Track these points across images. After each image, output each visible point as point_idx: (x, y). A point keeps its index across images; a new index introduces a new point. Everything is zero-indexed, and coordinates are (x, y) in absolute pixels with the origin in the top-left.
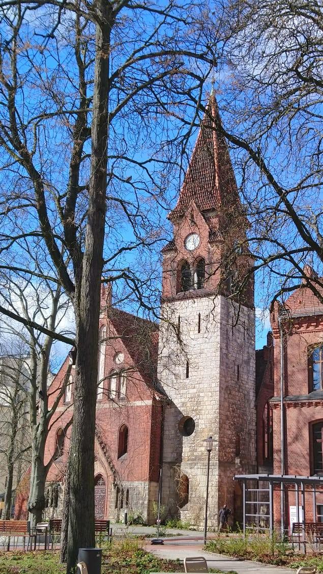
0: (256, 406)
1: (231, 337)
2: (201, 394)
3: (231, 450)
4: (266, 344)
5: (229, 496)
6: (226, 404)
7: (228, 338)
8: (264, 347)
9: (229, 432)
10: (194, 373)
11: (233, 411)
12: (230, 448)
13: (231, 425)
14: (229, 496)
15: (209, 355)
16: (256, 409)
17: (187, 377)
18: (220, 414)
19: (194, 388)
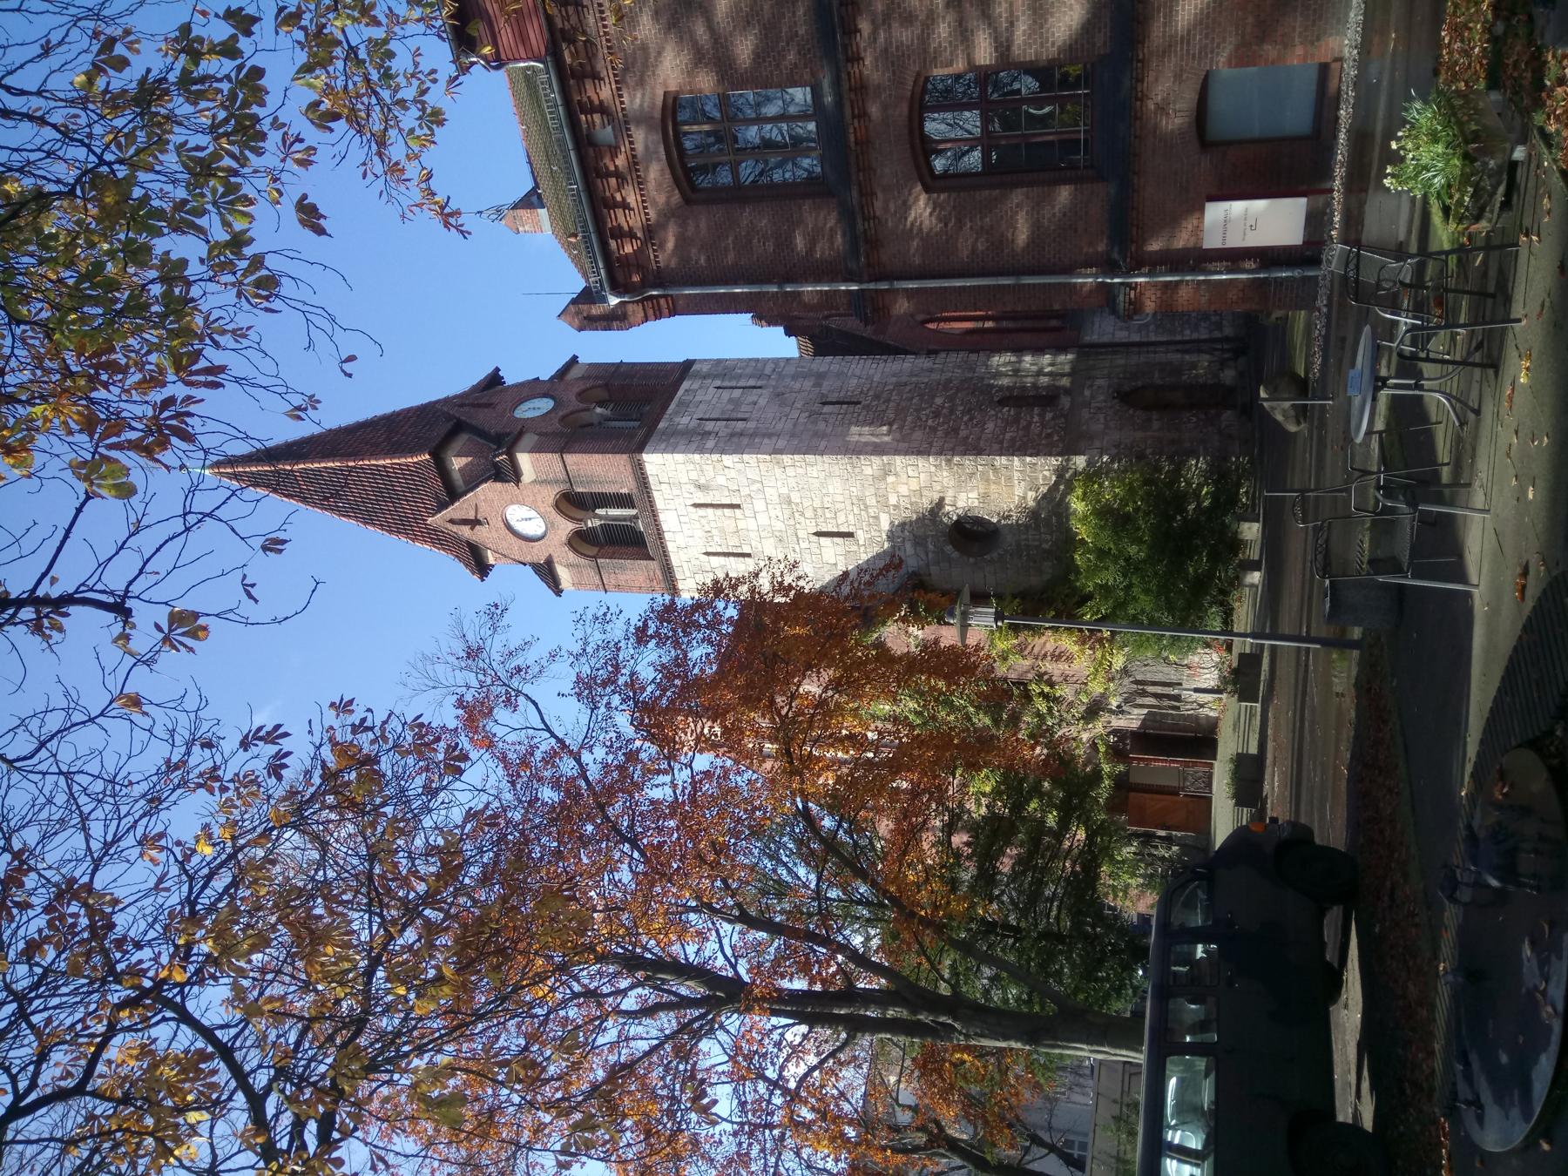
0: (931, 353)
1: (751, 425)
2: (893, 500)
3: (1036, 419)
4: (781, 330)
6: (918, 435)
7: (754, 435)
9: (990, 426)
10: (841, 518)
11: (937, 415)
12: (1030, 424)
13: (971, 419)
14: (1156, 425)
15: (792, 482)
16: (936, 352)
17: (850, 535)
18: (940, 453)
19: (877, 518)
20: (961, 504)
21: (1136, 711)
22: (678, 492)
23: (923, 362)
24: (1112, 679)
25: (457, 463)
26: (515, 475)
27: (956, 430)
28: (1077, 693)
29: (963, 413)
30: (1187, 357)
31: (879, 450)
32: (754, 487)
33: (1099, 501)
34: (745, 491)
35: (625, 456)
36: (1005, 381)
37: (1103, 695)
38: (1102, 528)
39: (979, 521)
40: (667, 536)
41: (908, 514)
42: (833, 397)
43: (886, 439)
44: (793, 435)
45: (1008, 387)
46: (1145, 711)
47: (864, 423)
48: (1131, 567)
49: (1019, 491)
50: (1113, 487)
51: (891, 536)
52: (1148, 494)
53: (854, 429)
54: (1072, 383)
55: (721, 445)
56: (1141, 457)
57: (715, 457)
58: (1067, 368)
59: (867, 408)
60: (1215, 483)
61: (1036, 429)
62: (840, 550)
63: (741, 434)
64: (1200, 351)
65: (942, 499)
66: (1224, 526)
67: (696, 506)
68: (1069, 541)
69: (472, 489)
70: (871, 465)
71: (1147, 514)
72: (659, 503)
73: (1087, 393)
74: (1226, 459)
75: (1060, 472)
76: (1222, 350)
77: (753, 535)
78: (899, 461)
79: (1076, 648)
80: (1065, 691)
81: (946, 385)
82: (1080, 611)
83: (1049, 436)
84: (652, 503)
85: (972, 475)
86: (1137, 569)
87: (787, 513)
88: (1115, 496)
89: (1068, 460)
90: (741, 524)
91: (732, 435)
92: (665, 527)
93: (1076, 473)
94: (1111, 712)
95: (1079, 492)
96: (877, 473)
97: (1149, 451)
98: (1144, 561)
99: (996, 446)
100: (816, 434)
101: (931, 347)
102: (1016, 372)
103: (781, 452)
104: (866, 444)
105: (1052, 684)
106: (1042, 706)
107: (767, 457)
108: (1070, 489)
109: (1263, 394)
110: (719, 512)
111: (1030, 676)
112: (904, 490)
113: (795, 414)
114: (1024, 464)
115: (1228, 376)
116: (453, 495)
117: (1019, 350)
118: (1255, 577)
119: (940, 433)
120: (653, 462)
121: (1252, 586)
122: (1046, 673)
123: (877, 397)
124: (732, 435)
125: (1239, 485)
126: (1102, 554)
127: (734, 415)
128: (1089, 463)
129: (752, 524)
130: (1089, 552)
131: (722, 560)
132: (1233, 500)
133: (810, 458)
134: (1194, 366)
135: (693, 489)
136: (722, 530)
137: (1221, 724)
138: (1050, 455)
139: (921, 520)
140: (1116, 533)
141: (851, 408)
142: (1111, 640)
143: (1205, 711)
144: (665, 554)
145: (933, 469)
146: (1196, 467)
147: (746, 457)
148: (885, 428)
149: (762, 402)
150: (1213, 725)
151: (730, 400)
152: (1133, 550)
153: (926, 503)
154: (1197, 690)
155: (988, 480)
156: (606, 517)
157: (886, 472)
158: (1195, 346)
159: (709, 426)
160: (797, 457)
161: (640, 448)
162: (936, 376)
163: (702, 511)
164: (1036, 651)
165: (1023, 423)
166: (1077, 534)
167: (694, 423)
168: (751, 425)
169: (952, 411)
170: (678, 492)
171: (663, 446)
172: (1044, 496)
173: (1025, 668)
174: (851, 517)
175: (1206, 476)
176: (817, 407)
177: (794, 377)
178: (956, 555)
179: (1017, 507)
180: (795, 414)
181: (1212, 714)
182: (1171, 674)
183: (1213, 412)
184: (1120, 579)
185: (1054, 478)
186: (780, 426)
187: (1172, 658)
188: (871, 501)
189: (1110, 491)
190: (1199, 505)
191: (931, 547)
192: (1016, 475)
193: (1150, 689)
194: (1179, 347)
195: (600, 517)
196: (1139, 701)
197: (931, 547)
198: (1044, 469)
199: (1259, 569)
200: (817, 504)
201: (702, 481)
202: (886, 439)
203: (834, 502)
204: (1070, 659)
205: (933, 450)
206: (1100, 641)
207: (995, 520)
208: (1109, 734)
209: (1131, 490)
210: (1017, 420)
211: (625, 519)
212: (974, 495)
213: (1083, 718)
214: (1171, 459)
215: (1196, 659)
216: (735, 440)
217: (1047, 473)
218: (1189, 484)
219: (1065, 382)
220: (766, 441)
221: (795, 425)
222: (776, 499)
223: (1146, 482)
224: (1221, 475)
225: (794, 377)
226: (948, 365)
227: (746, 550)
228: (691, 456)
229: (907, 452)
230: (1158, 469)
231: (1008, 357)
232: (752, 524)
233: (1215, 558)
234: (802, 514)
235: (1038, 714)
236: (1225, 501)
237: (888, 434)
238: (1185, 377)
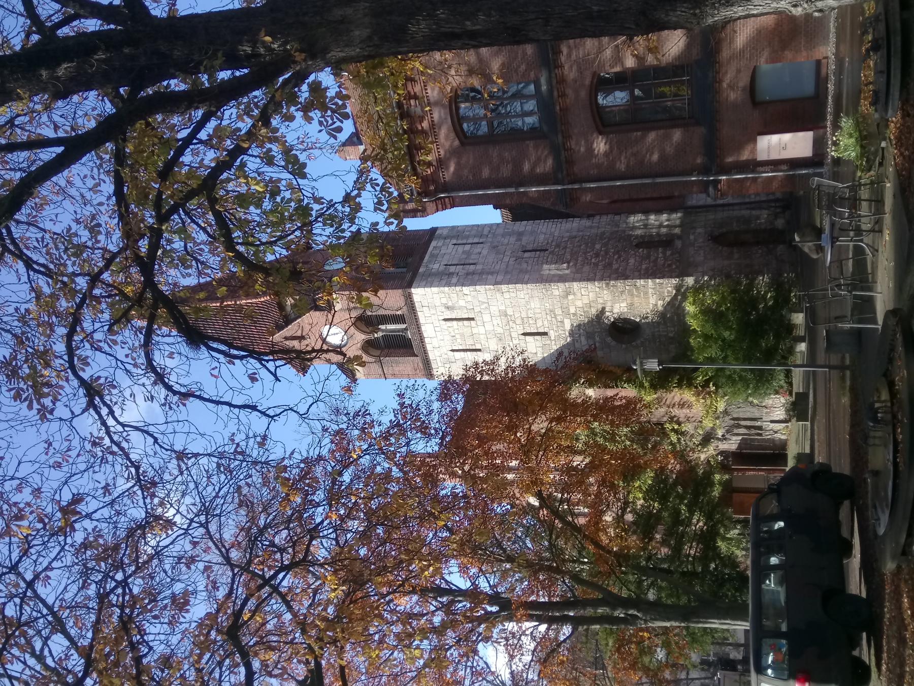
0: (590, 216)
1: (479, 267)
2: (572, 310)
5: (736, 256)
6: (586, 268)
7: (481, 273)
8: (496, 207)
9: (632, 261)
10: (539, 323)
11: (597, 255)
12: (657, 258)
13: (619, 257)
14: (736, 256)
15: (508, 302)
16: (593, 216)
17: (545, 334)
18: (601, 279)
19: (562, 322)
20: (615, 311)
21: (734, 438)
22: (434, 312)
23: (585, 222)
24: (718, 418)
25: (290, 301)
26: (330, 307)
27: (610, 265)
28: (696, 428)
29: (614, 254)
30: (754, 212)
31: (562, 279)
32: (483, 307)
33: (703, 305)
34: (477, 309)
35: (400, 291)
36: (639, 232)
37: (713, 428)
38: (707, 321)
39: (626, 321)
40: (426, 340)
41: (582, 318)
42: (530, 247)
43: (567, 272)
44: (506, 273)
45: (642, 236)
46: (740, 438)
47: (551, 263)
48: (726, 345)
49: (652, 301)
50: (712, 295)
51: (572, 333)
52: (734, 299)
53: (545, 267)
54: (682, 231)
55: (461, 280)
56: (728, 276)
57: (458, 288)
58: (678, 222)
59: (552, 253)
60: (775, 290)
61: (661, 261)
62: (539, 344)
63: (473, 273)
64: (760, 208)
65: (603, 309)
66: (782, 315)
67: (445, 320)
68: (686, 331)
69: (300, 317)
70: (557, 289)
71: (734, 311)
72: (422, 320)
73: (692, 237)
74: (781, 275)
75: (678, 288)
76: (776, 207)
77: (482, 337)
78: (575, 285)
79: (694, 398)
80: (688, 427)
81: (602, 236)
82: (695, 375)
83: (670, 265)
84: (417, 320)
85: (622, 292)
86: (730, 346)
87: (505, 321)
88: (714, 301)
89: (682, 280)
90: (475, 331)
91: (468, 274)
92: (425, 335)
93: (688, 288)
94: (719, 439)
95: (691, 299)
96: (562, 294)
97: (733, 272)
98: (734, 341)
99: (637, 274)
100: (521, 271)
101: (590, 212)
102: (646, 226)
103: (500, 283)
104: (554, 275)
105: (679, 424)
106: (674, 438)
107: (492, 287)
108: (685, 298)
109: (797, 239)
110: (460, 323)
111: (665, 419)
112: (579, 304)
113: (506, 259)
114: (655, 284)
115: (780, 223)
116: (288, 321)
117: (646, 212)
118: (802, 347)
119: (600, 267)
120: (419, 294)
121: (801, 352)
122: (675, 416)
123: (558, 246)
124: (468, 274)
125: (790, 292)
126: (707, 337)
127: (467, 261)
128: (696, 281)
129: (482, 330)
130: (699, 337)
131: (462, 353)
132: (787, 300)
133: (519, 286)
134: (758, 218)
135: (444, 310)
136: (462, 335)
137: (789, 443)
138: (671, 277)
139: (591, 322)
140: (715, 324)
141: (542, 254)
142: (716, 392)
143: (778, 436)
144: (425, 352)
145: (597, 290)
146: (763, 281)
147: (478, 287)
148: (565, 265)
149: (485, 252)
150: (783, 445)
151: (464, 252)
152: (726, 334)
153: (594, 311)
154: (772, 422)
155: (632, 295)
156: (386, 330)
157: (567, 294)
158: (758, 205)
159: (452, 269)
160: (510, 286)
161: (410, 286)
162: (594, 231)
163: (449, 324)
164: (668, 402)
165: (652, 258)
166: (691, 326)
167: (442, 268)
168: (479, 267)
169: (607, 253)
170: (434, 312)
171: (424, 283)
172: (669, 303)
173: (662, 414)
174: (546, 323)
175: (770, 285)
176: (520, 254)
177: (503, 236)
178: (613, 343)
179: (652, 311)
180: (506, 259)
181: (783, 437)
182: (756, 413)
183: (771, 246)
184: (719, 353)
185: (674, 292)
186: (497, 267)
187: (755, 401)
188: (558, 312)
189: (710, 298)
190: (766, 305)
191: (597, 339)
192: (650, 290)
193: (743, 423)
194: (748, 206)
195: (383, 331)
196: (736, 431)
197: (597, 339)
198: (668, 286)
199: (804, 341)
200: (524, 315)
201: (450, 304)
202: (567, 272)
203: (534, 314)
204: (690, 407)
205: (597, 277)
206: (709, 393)
207: (638, 320)
208: (717, 455)
209: (723, 298)
210: (648, 257)
211: (399, 331)
212: (624, 305)
213: (700, 444)
214: (747, 277)
215: (770, 402)
216: (470, 277)
217: (670, 289)
218: (759, 292)
219: (677, 231)
220: (490, 277)
221: (507, 266)
222: (497, 313)
223: (733, 291)
224: (778, 285)
225: (503, 236)
226: (603, 224)
227: (478, 347)
228: (442, 289)
229: (581, 280)
230: (739, 283)
231: (640, 217)
232: (482, 330)
233: (778, 337)
234: (514, 322)
235: (671, 444)
236: (783, 302)
237: (568, 268)
238: (753, 225)
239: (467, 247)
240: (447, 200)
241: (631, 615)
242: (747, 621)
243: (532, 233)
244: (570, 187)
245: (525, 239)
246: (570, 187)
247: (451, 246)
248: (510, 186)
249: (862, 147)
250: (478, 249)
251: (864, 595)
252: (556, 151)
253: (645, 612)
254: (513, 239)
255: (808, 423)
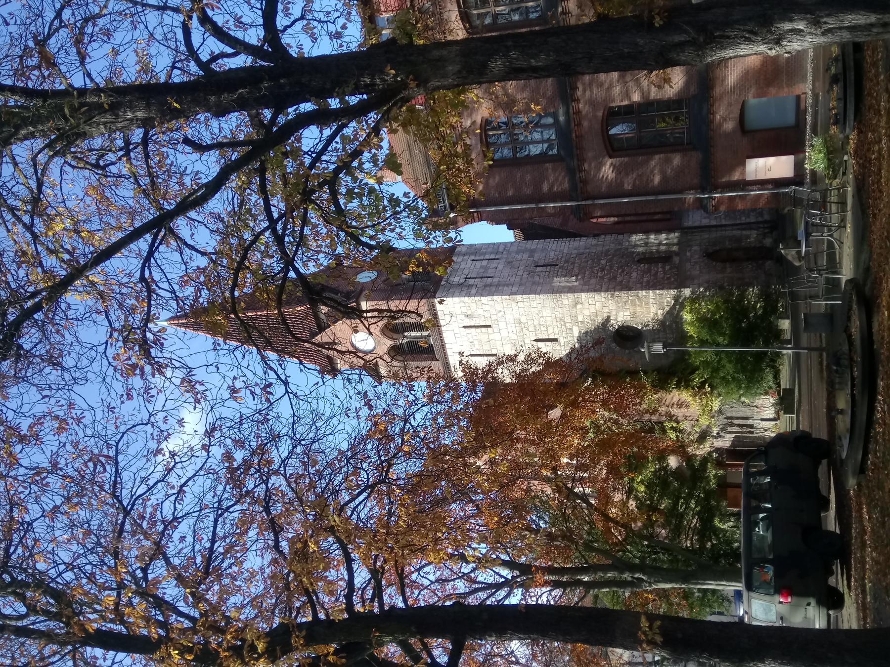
0: (595, 236)
1: (496, 280)
2: (580, 318)
3: (660, 269)
5: (729, 270)
6: (593, 281)
7: (498, 285)
8: (509, 228)
9: (634, 274)
10: (550, 330)
11: (603, 270)
12: (657, 272)
13: (623, 271)
14: (729, 270)
15: (522, 311)
17: (555, 340)
18: (607, 290)
19: (571, 329)
20: (619, 319)
21: (728, 436)
23: (592, 241)
24: (713, 417)
27: (615, 278)
28: (693, 426)
29: (618, 268)
30: (744, 232)
31: (571, 290)
32: (500, 314)
33: (699, 313)
34: (494, 317)
36: (640, 249)
37: (708, 427)
38: (702, 327)
40: (447, 346)
41: (589, 326)
42: (542, 262)
43: (575, 284)
44: (521, 285)
46: (733, 435)
47: (561, 276)
49: (653, 310)
50: (707, 305)
51: (580, 340)
52: (727, 308)
53: (556, 279)
55: (480, 291)
56: (721, 288)
57: (477, 298)
58: (676, 241)
59: (562, 267)
61: (660, 275)
63: (491, 285)
64: (751, 229)
65: (609, 317)
66: (771, 322)
67: (465, 327)
70: (567, 299)
71: (727, 319)
73: (688, 254)
74: (769, 287)
75: (676, 298)
76: (764, 228)
78: (583, 295)
79: (691, 399)
80: (686, 425)
81: (607, 253)
82: (692, 377)
83: (669, 278)
85: (626, 302)
87: (519, 329)
88: (709, 310)
89: (680, 292)
90: (491, 337)
91: (485, 286)
92: (446, 340)
94: (714, 437)
95: (688, 308)
96: (571, 304)
99: (639, 285)
100: (534, 283)
101: (596, 232)
102: (646, 244)
104: (564, 287)
105: (678, 422)
107: (508, 297)
108: (682, 307)
110: (479, 330)
112: (587, 312)
113: (520, 273)
115: (768, 242)
116: (322, 328)
117: (647, 232)
119: (606, 280)
123: (567, 261)
124: (485, 286)
125: (778, 302)
127: (485, 275)
128: (693, 292)
132: (775, 310)
133: (532, 296)
134: (748, 237)
135: (463, 317)
139: (597, 329)
140: (710, 330)
141: (553, 268)
142: (711, 393)
144: (446, 357)
145: (603, 300)
146: (752, 292)
147: (495, 298)
149: (501, 267)
151: (481, 267)
153: (600, 320)
154: (762, 420)
155: (635, 305)
156: (411, 337)
157: (576, 304)
158: (749, 226)
159: (471, 282)
160: (524, 296)
162: (600, 249)
163: (468, 330)
164: (667, 403)
165: (653, 272)
167: (462, 281)
168: (496, 280)
169: (611, 267)
172: (668, 312)
174: (556, 330)
175: (759, 296)
176: (533, 268)
177: (518, 252)
178: (618, 349)
180: (520, 273)
182: (747, 412)
183: (760, 262)
186: (512, 280)
187: (747, 401)
188: (568, 320)
189: (705, 308)
190: (756, 313)
193: (736, 422)
196: (729, 429)
198: (667, 297)
200: (536, 323)
201: (469, 313)
202: (575, 284)
204: (687, 406)
206: (705, 394)
210: (649, 271)
212: (627, 313)
214: (738, 288)
215: (761, 402)
218: (749, 302)
219: (675, 248)
220: (506, 288)
223: (726, 301)
224: (768, 297)
225: (518, 252)
226: (607, 242)
231: (640, 236)
234: (528, 329)
236: (771, 310)
239: (485, 263)
240: (475, 215)
241: (636, 578)
242: (740, 582)
243: (543, 250)
244: (583, 203)
245: (536, 256)
246: (583, 203)
247: (469, 262)
248: (531, 203)
249: (829, 160)
250: (494, 264)
251: (838, 531)
252: (572, 173)
253: (650, 576)
254: (526, 256)
255: (794, 416)
